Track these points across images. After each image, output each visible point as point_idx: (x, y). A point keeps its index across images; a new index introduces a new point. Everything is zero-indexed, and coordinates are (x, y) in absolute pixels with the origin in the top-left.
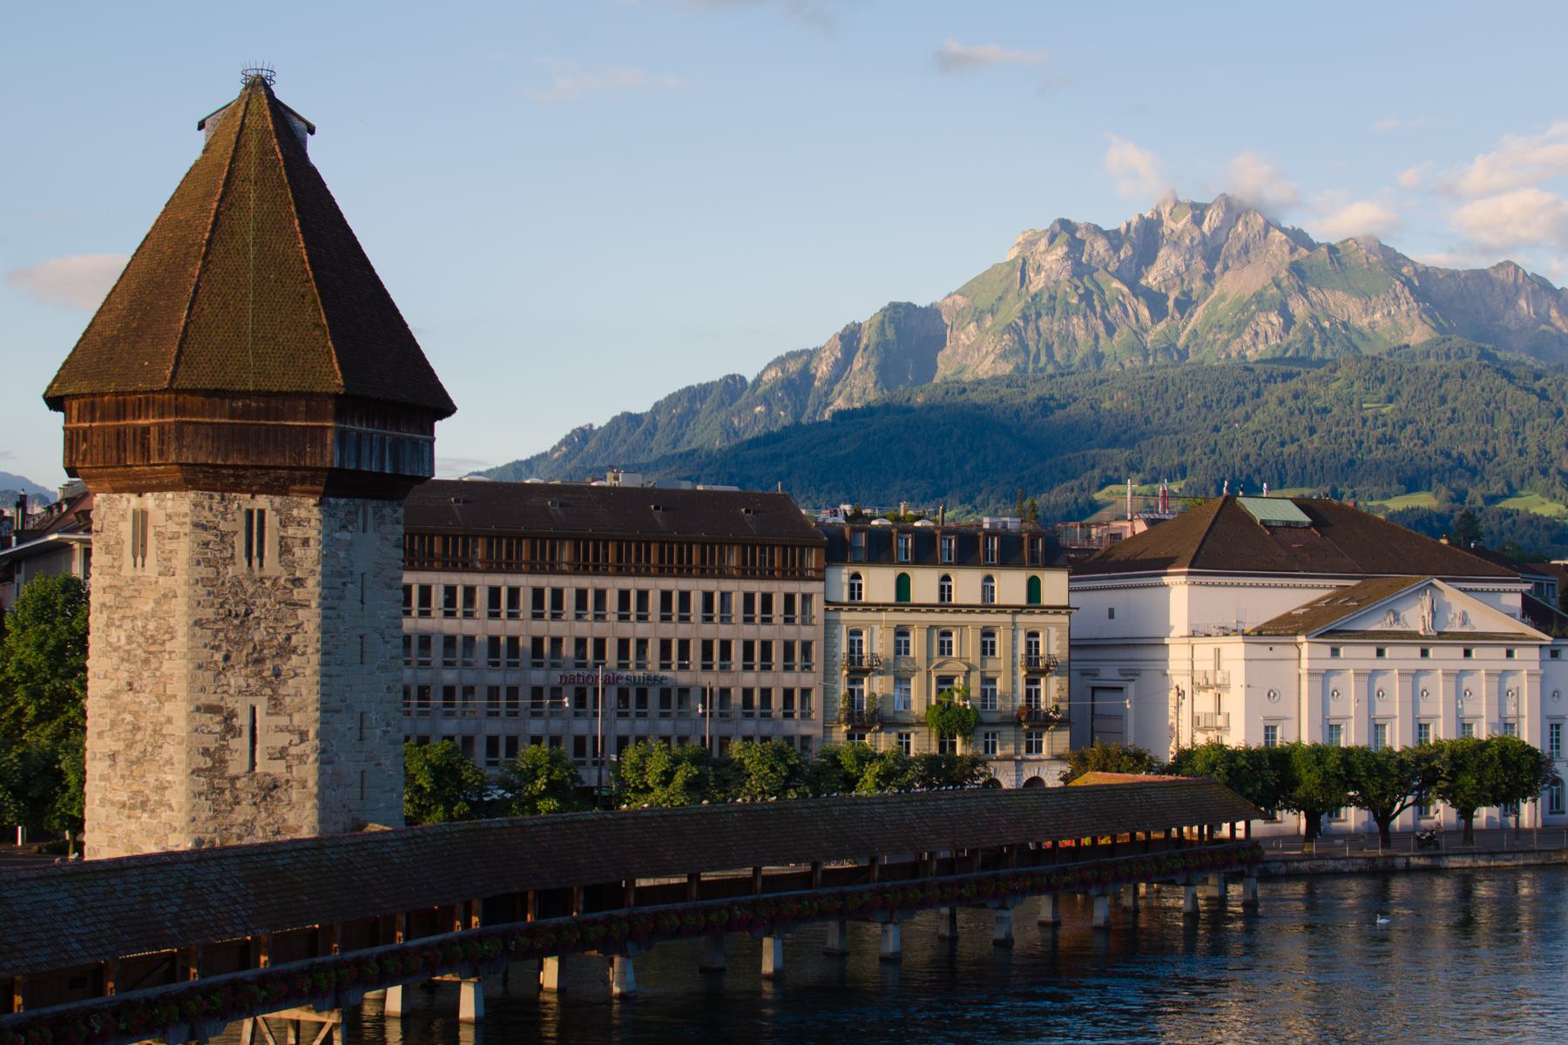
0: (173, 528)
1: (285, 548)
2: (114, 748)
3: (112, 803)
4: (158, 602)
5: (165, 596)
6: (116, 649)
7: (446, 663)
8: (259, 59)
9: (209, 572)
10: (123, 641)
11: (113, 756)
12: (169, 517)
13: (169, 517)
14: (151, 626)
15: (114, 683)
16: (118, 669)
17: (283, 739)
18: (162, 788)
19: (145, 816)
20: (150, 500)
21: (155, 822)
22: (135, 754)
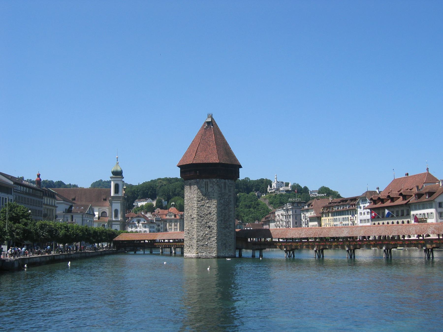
3: (222, 228)
4: (228, 196)
5: (229, 195)
6: (222, 203)
10: (223, 202)
11: (221, 220)
12: (230, 183)
13: (230, 183)
14: (227, 200)
15: (222, 209)
16: (222, 207)
18: (230, 225)
19: (227, 229)
20: (227, 181)
21: (229, 230)
22: (225, 220)
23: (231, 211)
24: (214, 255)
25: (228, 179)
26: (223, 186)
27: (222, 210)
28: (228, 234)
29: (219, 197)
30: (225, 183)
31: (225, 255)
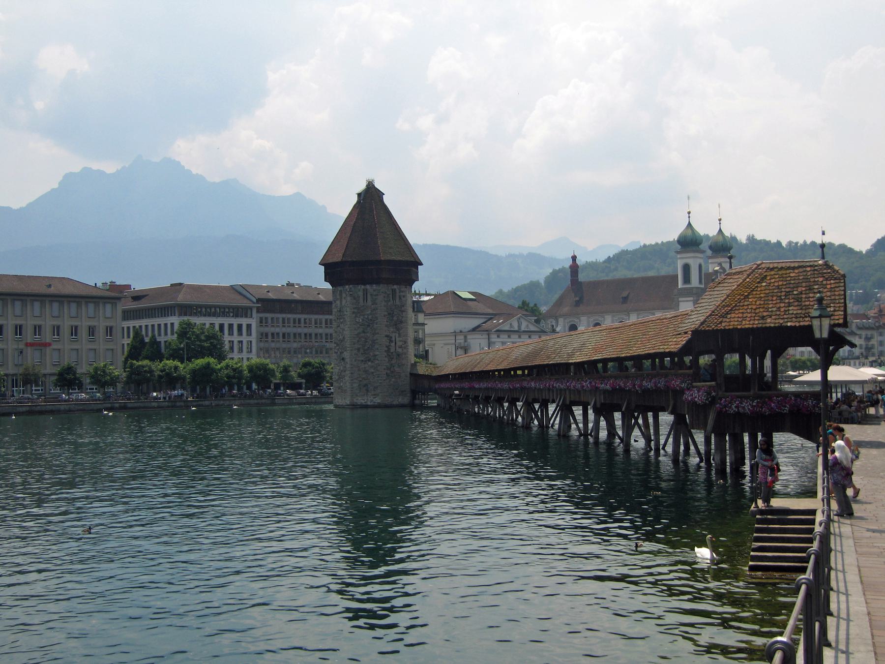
0: (375, 293)
1: (400, 298)
2: (359, 347)
4: (372, 311)
5: (374, 310)
6: (358, 323)
7: (272, 341)
8: (370, 178)
9: (386, 304)
11: (359, 349)
13: (374, 290)
14: (370, 317)
16: (359, 328)
17: (401, 343)
18: (375, 356)
19: (370, 363)
20: (368, 287)
23: (378, 333)
24: (348, 403)
25: (371, 283)
26: (361, 296)
27: (360, 333)
28: (373, 371)
29: (354, 313)
30: (365, 292)
31: (365, 402)
